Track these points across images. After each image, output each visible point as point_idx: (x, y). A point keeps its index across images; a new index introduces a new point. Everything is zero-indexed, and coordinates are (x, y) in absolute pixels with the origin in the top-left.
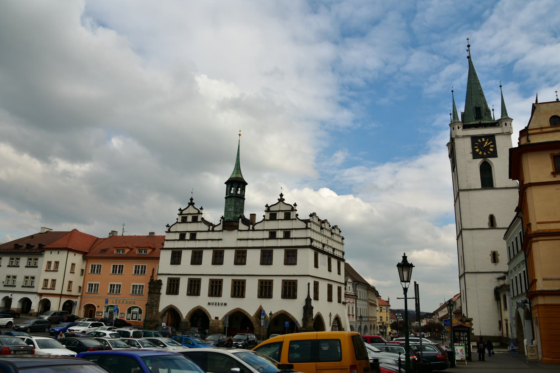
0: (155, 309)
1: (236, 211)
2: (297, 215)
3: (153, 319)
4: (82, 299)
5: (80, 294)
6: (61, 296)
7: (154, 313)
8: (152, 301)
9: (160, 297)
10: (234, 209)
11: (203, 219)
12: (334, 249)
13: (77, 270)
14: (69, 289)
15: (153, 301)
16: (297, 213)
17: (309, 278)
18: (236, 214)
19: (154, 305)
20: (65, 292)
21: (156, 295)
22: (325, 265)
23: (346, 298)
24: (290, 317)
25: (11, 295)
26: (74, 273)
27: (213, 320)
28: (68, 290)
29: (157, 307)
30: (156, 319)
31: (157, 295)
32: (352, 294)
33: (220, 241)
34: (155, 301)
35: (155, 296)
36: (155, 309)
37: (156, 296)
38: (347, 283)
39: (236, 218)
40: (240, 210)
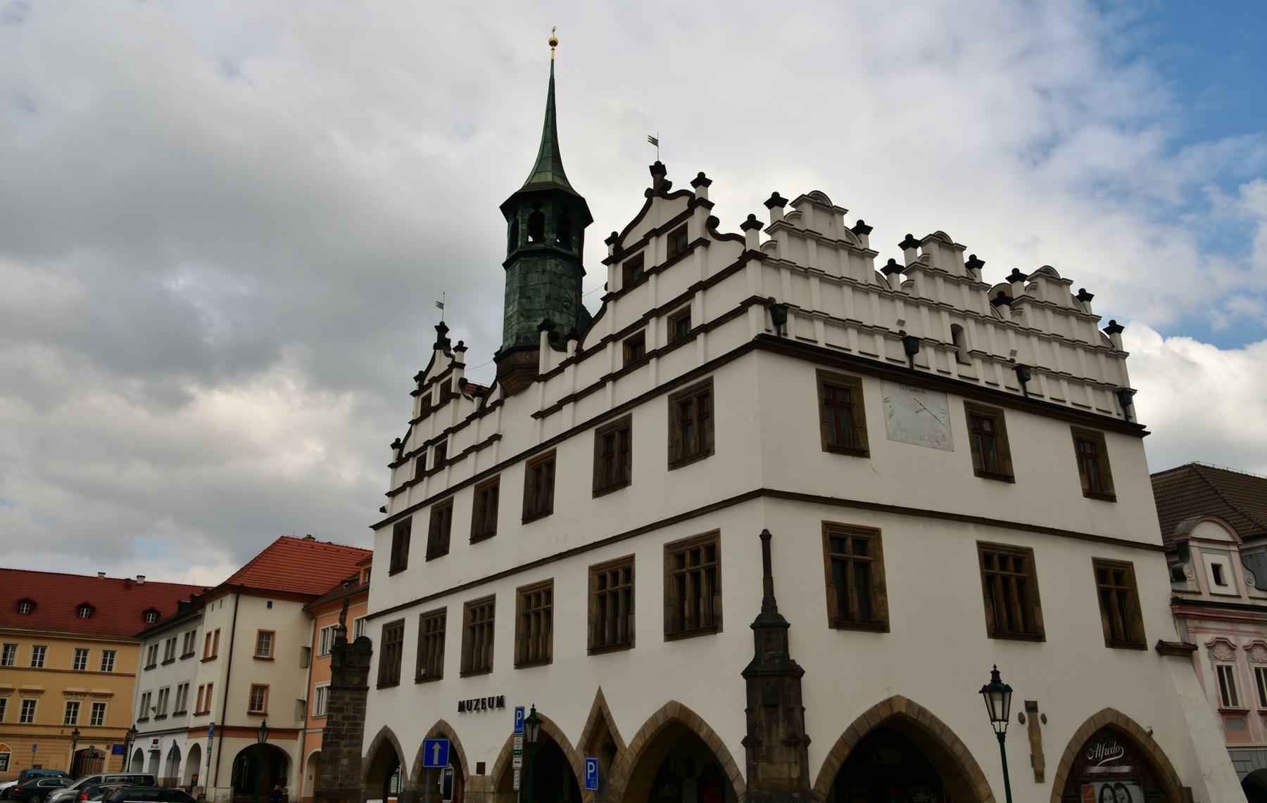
0: (346, 746)
1: (528, 307)
2: (713, 222)
3: (340, 785)
4: (307, 736)
5: (302, 725)
6: (221, 730)
7: (345, 762)
8: (334, 719)
9: (365, 700)
10: (519, 303)
11: (463, 382)
12: (1023, 373)
13: (286, 648)
14: (260, 708)
15: (338, 717)
16: (714, 212)
17: (761, 504)
18: (528, 318)
19: (344, 733)
20: (239, 716)
21: (347, 696)
22: (941, 442)
23: (1191, 623)
24: (702, 734)
25: (156, 742)
26: (271, 660)
27: (472, 776)
28: (249, 714)
29: (354, 741)
30: (350, 787)
31: (356, 695)
32: (1246, 601)
33: (495, 443)
34: (344, 718)
35: (347, 700)
36: (346, 750)
37: (351, 699)
38: (1191, 543)
39: (529, 335)
40: (548, 298)
